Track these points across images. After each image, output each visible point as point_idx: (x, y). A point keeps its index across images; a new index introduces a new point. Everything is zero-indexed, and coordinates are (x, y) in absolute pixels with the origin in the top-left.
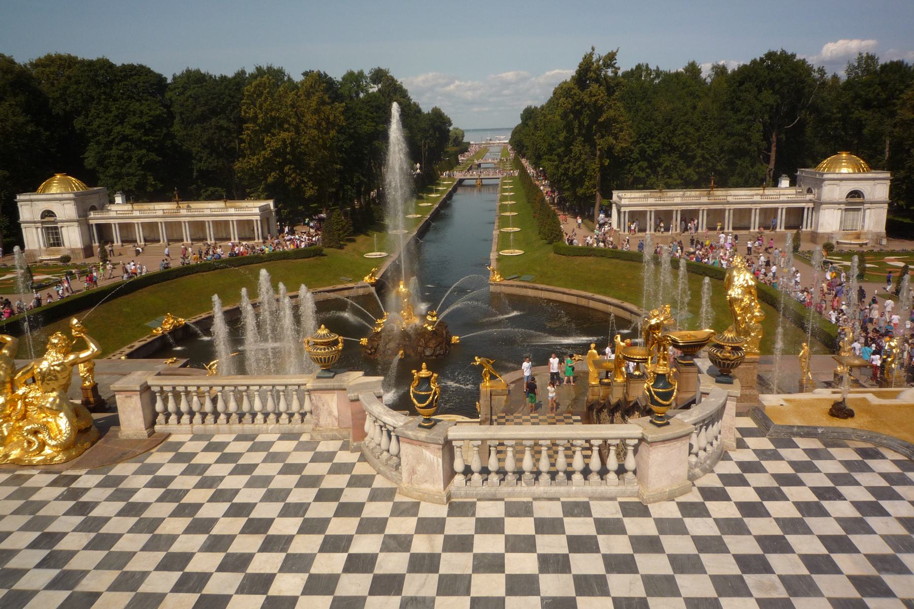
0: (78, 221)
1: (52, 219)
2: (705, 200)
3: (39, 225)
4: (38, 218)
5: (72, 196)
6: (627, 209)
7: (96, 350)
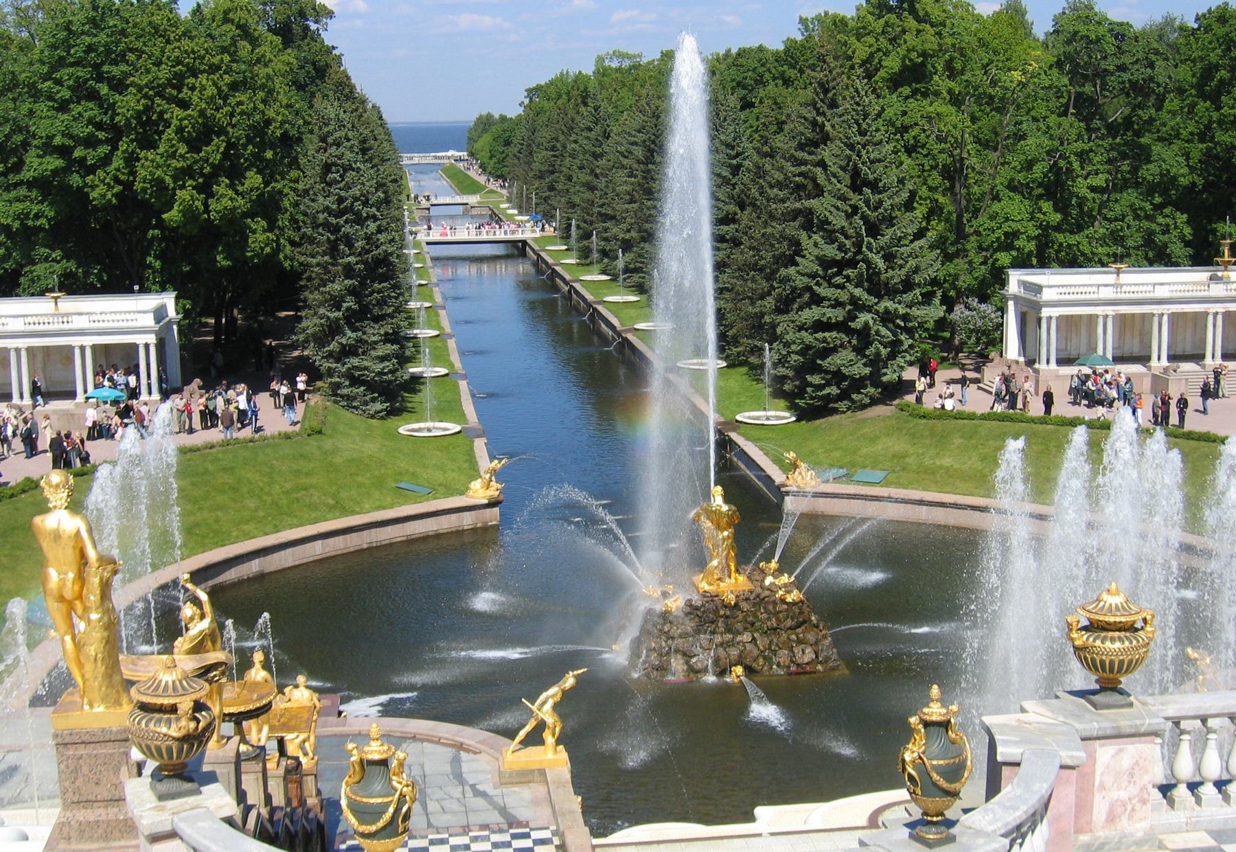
2: (1218, 290)
6: (1056, 312)
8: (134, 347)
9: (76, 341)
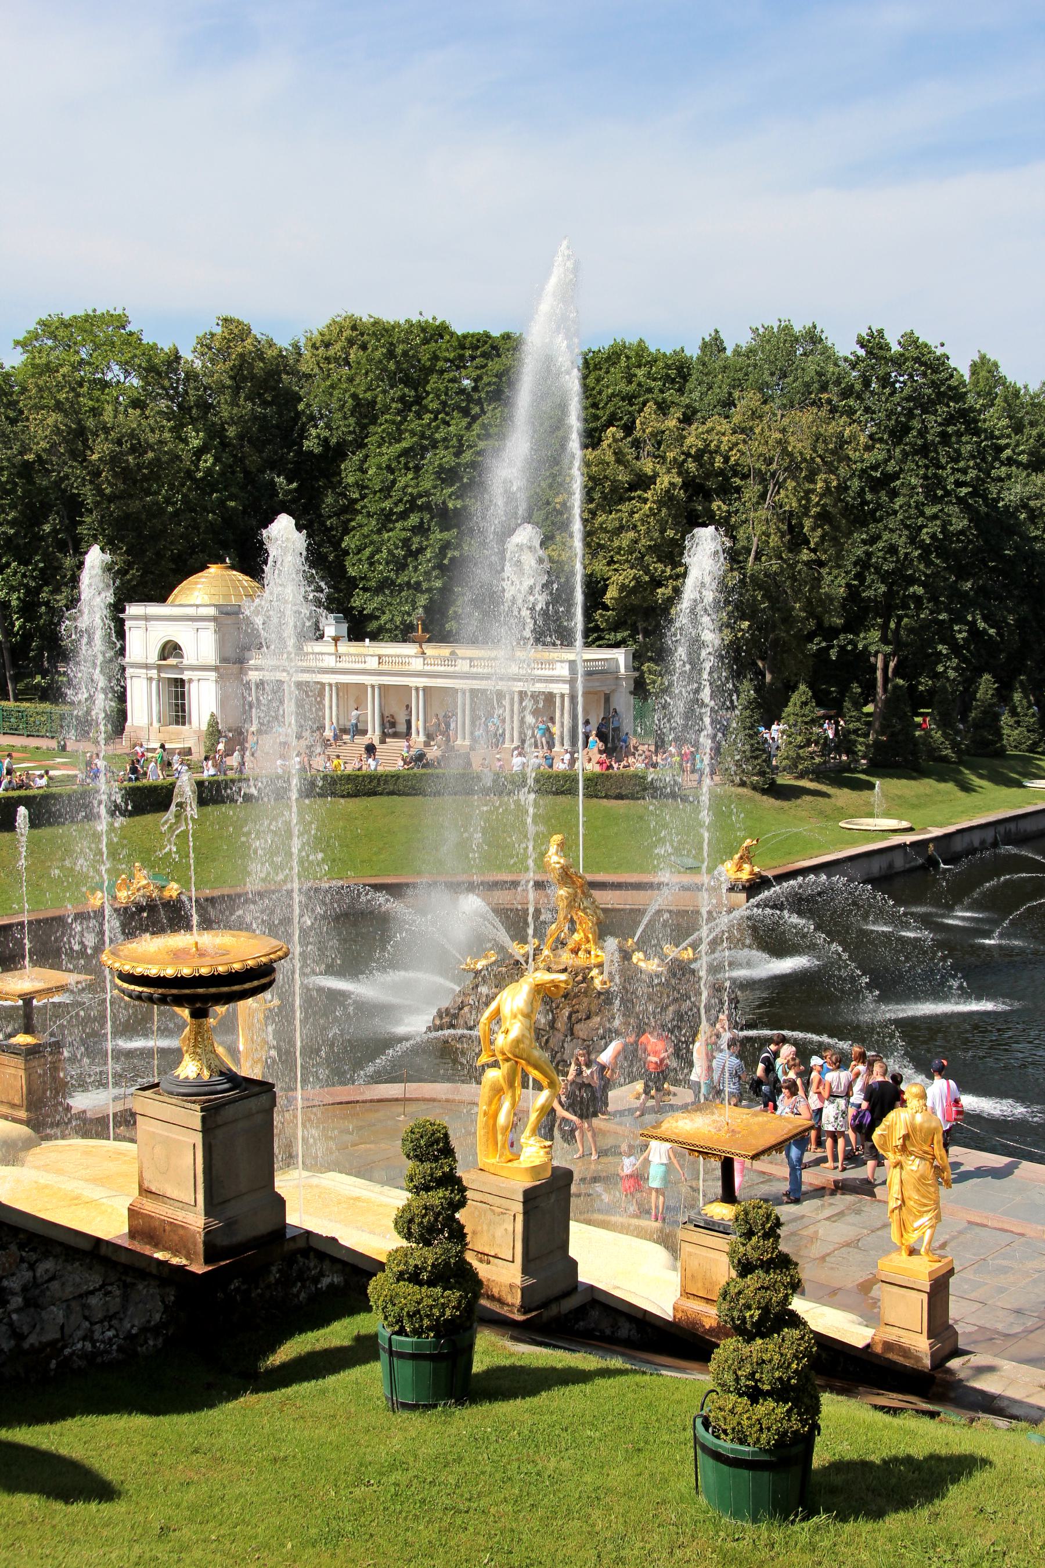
0: (216, 669)
1: (172, 661)
3: (153, 673)
4: (153, 658)
5: (212, 611)
8: (550, 697)
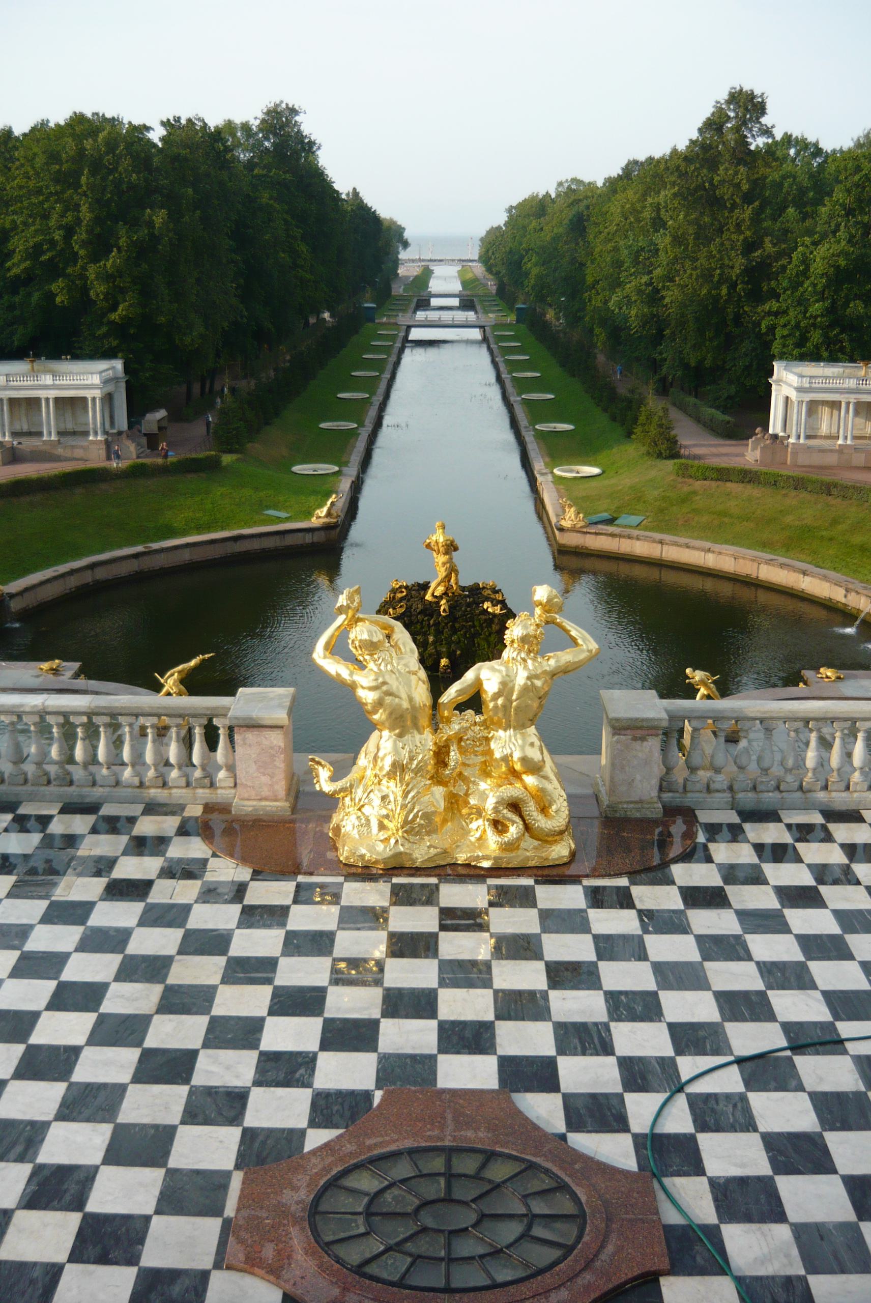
7: (594, 646)
8: (84, 399)
9: (42, 394)
